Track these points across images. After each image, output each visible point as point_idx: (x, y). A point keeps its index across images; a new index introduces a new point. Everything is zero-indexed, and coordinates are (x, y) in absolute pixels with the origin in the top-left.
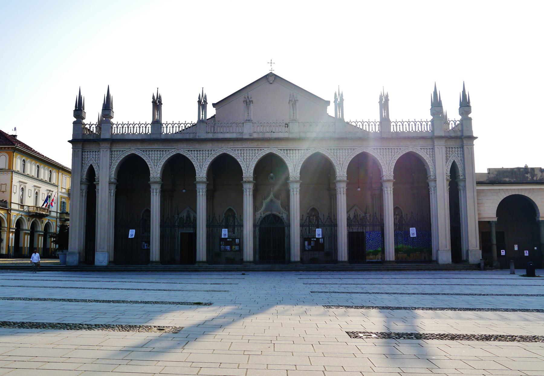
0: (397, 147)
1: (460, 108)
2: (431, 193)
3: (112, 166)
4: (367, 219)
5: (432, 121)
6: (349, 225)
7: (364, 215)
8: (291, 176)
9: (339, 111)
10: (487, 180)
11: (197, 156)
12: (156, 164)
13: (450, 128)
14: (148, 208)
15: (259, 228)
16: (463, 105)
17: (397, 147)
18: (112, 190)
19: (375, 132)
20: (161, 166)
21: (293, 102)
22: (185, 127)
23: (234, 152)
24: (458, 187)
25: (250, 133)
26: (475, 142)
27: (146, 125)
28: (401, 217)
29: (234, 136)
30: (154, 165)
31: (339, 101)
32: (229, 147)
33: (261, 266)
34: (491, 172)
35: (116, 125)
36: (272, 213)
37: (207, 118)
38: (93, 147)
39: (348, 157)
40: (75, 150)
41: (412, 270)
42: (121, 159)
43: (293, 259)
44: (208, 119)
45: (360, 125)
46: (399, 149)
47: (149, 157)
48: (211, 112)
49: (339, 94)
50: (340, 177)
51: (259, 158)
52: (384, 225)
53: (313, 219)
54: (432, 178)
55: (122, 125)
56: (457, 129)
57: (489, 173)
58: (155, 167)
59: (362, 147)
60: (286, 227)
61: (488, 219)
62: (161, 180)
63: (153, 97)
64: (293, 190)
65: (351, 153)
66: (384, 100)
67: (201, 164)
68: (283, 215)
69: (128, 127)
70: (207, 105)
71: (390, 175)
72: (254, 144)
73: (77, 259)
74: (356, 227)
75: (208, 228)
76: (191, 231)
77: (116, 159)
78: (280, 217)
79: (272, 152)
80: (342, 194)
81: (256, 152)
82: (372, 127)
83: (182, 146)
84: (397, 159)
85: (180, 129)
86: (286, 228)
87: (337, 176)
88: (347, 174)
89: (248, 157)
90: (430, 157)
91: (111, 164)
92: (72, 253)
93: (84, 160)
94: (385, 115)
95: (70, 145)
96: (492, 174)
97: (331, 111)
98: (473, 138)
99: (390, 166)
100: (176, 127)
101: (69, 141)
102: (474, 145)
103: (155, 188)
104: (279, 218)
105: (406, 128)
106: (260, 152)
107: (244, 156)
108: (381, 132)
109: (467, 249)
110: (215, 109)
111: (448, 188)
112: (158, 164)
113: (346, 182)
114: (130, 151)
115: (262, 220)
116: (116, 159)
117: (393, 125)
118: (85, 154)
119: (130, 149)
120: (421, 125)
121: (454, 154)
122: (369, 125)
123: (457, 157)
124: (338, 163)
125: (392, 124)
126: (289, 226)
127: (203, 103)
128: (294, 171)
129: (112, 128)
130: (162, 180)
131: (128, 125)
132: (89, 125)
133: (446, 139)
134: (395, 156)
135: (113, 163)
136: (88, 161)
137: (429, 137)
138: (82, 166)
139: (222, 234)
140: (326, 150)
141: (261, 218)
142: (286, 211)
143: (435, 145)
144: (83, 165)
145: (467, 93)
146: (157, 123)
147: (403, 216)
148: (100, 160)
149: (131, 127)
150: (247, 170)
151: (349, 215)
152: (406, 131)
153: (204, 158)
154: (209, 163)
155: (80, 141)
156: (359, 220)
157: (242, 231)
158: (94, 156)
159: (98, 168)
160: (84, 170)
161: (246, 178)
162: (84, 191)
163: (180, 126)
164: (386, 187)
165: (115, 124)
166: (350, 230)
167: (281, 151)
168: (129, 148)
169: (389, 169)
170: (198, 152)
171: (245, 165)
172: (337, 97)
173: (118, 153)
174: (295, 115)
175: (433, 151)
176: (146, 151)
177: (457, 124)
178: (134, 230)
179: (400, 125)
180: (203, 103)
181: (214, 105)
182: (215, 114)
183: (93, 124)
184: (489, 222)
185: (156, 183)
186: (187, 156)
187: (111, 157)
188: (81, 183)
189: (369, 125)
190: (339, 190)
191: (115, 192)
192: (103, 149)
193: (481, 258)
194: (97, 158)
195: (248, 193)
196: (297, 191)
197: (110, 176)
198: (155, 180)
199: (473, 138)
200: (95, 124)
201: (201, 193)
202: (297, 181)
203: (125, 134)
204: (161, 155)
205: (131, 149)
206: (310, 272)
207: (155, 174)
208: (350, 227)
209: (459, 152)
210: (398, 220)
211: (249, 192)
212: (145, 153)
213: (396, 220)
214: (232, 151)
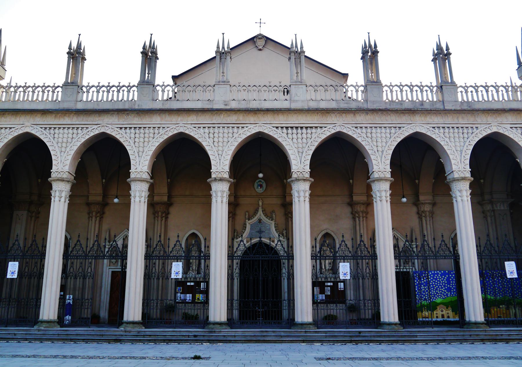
0: (472, 126)
8: (296, 171)
17: (472, 126)
20: (72, 152)
25: (225, 101)
29: (199, 105)
39: (391, 139)
46: (474, 128)
50: (380, 173)
59: (413, 125)
64: (299, 194)
72: (233, 118)
75: (148, 261)
79: (262, 131)
80: (384, 202)
83: (111, 121)
99: (463, 154)
103: (59, 189)
106: (241, 131)
107: (214, 137)
113: (391, 181)
114: (23, 129)
124: (375, 149)
128: (299, 162)
134: (469, 140)
139: (173, 272)
140: (354, 128)
150: (218, 161)
154: (154, 148)
164: (459, 190)
167: (276, 130)
169: (463, 160)
170: (137, 131)
171: (216, 152)
174: (299, 74)
178: (17, 263)
186: (118, 137)
190: (378, 195)
195: (219, 200)
196: (305, 197)
198: (59, 176)
201: (137, 199)
204: (75, 136)
205: (23, 125)
207: (60, 166)
211: (222, 197)
214: (194, 128)
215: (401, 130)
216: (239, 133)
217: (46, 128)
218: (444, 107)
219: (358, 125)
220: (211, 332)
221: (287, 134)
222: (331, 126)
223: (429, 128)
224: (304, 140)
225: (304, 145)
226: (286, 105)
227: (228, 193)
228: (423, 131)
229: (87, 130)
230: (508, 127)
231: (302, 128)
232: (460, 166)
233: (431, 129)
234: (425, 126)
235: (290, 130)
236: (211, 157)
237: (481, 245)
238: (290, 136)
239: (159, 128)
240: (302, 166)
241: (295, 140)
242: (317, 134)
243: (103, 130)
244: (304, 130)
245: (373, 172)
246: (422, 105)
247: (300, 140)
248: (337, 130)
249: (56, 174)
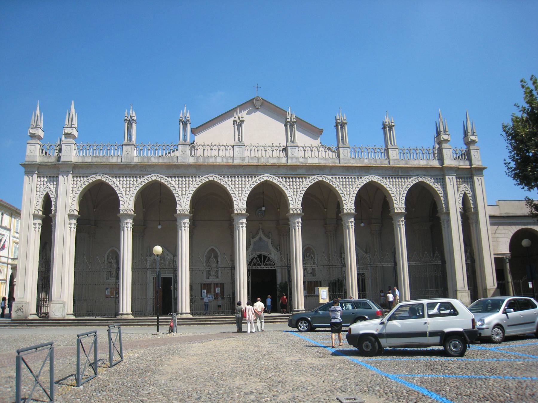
2: (444, 227)
99: (401, 196)
207: (126, 205)
221: (286, 182)
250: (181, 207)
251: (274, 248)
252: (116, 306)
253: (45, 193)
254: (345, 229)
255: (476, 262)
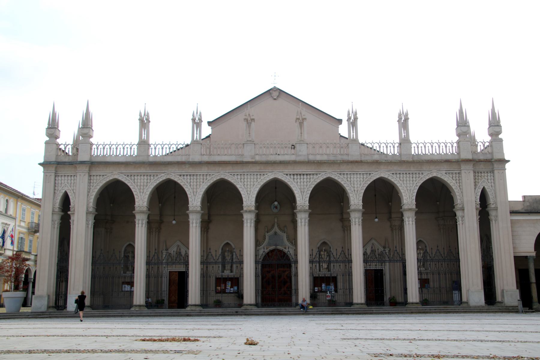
0: (419, 172)
1: (489, 127)
2: (459, 224)
3: (90, 192)
4: (386, 253)
5: (458, 142)
6: (366, 261)
7: (383, 249)
9: (353, 131)
10: (522, 209)
11: (191, 182)
12: (142, 191)
13: (479, 151)
14: (132, 243)
15: (261, 265)
16: (493, 124)
17: (419, 172)
18: (90, 220)
19: (394, 155)
20: (148, 193)
21: (301, 120)
22: (177, 148)
23: (233, 177)
24: (489, 217)
26: (507, 166)
27: (131, 146)
28: (425, 252)
29: (233, 158)
30: (140, 192)
31: (352, 120)
32: (227, 171)
33: (264, 310)
34: (526, 199)
35: (96, 145)
36: (277, 248)
37: (202, 138)
38: (68, 171)
40: (47, 174)
41: (440, 312)
42: (101, 185)
43: (355, 301)
44: (203, 139)
45: (376, 147)
46: (421, 173)
47: (134, 182)
48: (206, 131)
49: (353, 112)
51: (262, 183)
52: (406, 260)
53: (324, 254)
54: (460, 206)
55: (103, 145)
56: (486, 151)
57: (524, 201)
58: (141, 194)
60: (293, 263)
61: (525, 254)
62: (148, 209)
63: (140, 113)
65: (367, 179)
66: (403, 119)
67: (195, 190)
68: (289, 250)
69: (110, 148)
70: (202, 123)
71: (412, 203)
72: (257, 168)
73: (46, 303)
74: (374, 263)
76: (182, 269)
77: (95, 185)
78: (286, 253)
79: (276, 177)
80: (357, 225)
81: (259, 177)
82: (390, 149)
84: (419, 184)
85: (171, 151)
86: (293, 265)
87: (351, 204)
88: (480, 201)
89: (249, 183)
90: (456, 183)
91: (89, 191)
92: (41, 297)
93: (57, 185)
94: (404, 136)
95: (41, 168)
96: (528, 202)
97: (343, 130)
98: (505, 162)
99: (412, 192)
100: (166, 148)
101: (40, 164)
102: (506, 169)
104: (284, 253)
105: (428, 151)
106: (262, 177)
108: (400, 154)
109: (502, 289)
110: (210, 127)
111: (478, 218)
112: (145, 191)
113: (362, 211)
114: (112, 176)
115: (265, 256)
116: (96, 184)
117: (414, 147)
118: (59, 180)
119: (112, 173)
120: (446, 147)
121: (484, 179)
122: (387, 147)
123: (486, 183)
125: (413, 146)
126: (296, 262)
127: (198, 121)
129: (91, 149)
130: (149, 210)
131: (111, 145)
132: (64, 145)
133: (474, 162)
135: (92, 189)
136: (61, 187)
137: (454, 161)
138: (55, 193)
141: (264, 253)
142: (293, 246)
143: (462, 169)
144: (56, 191)
145: (496, 112)
146: (144, 144)
147: (428, 251)
148: (76, 186)
149: (113, 148)
150: (248, 198)
151: (366, 249)
152: (443, 154)
153: (198, 183)
155: (54, 164)
156: (377, 256)
157: (242, 268)
158: (69, 181)
159: (74, 195)
160: (56, 197)
161: (247, 207)
162: (56, 223)
163: (170, 146)
164: (407, 217)
165: (94, 144)
166: (367, 267)
167: (286, 176)
168: (111, 172)
169: (411, 196)
171: (246, 192)
172: (350, 115)
173: (98, 177)
174: (302, 135)
175: (460, 176)
176: (131, 175)
177: (486, 146)
179: (421, 147)
180: (197, 121)
181: (210, 123)
182: (211, 133)
183: (69, 144)
184: (526, 257)
185: (250, 211)
187: (90, 182)
188: (53, 212)
189: (387, 147)
190: (354, 220)
191: (93, 223)
192: (80, 174)
193: (519, 299)
194: (72, 184)
196: (305, 223)
197: (88, 205)
198: (141, 209)
199: (505, 162)
200: (122, 144)
202: (305, 210)
203: (113, 155)
204: (149, 181)
206: (510, 313)
207: (141, 203)
208: (366, 264)
209: (489, 178)
210: (421, 255)
212: (129, 177)
213: (419, 254)
214: (230, 175)
215: (370, 176)
216: (261, 179)
217: (128, 176)
218: (401, 158)
219: (342, 173)
220: (246, 310)
221: (294, 179)
222: (323, 173)
223: (389, 174)
224: (305, 183)
225: (305, 187)
226: (293, 158)
227: (255, 219)
228: (386, 176)
229: (157, 177)
230: (443, 173)
231: (303, 175)
232: (409, 200)
233: (391, 175)
234: (387, 173)
235: (295, 177)
236: (243, 196)
237: (433, 253)
238: (295, 180)
239: (207, 175)
240: (304, 202)
241: (299, 183)
242: (314, 179)
243: (168, 177)
244: (305, 176)
245: (351, 205)
246: (387, 157)
247: (302, 183)
248: (328, 176)
249: (139, 208)
250: (193, 204)
251: (289, 242)
252: (131, 298)
253: (64, 191)
254: (352, 225)
255: (494, 260)
